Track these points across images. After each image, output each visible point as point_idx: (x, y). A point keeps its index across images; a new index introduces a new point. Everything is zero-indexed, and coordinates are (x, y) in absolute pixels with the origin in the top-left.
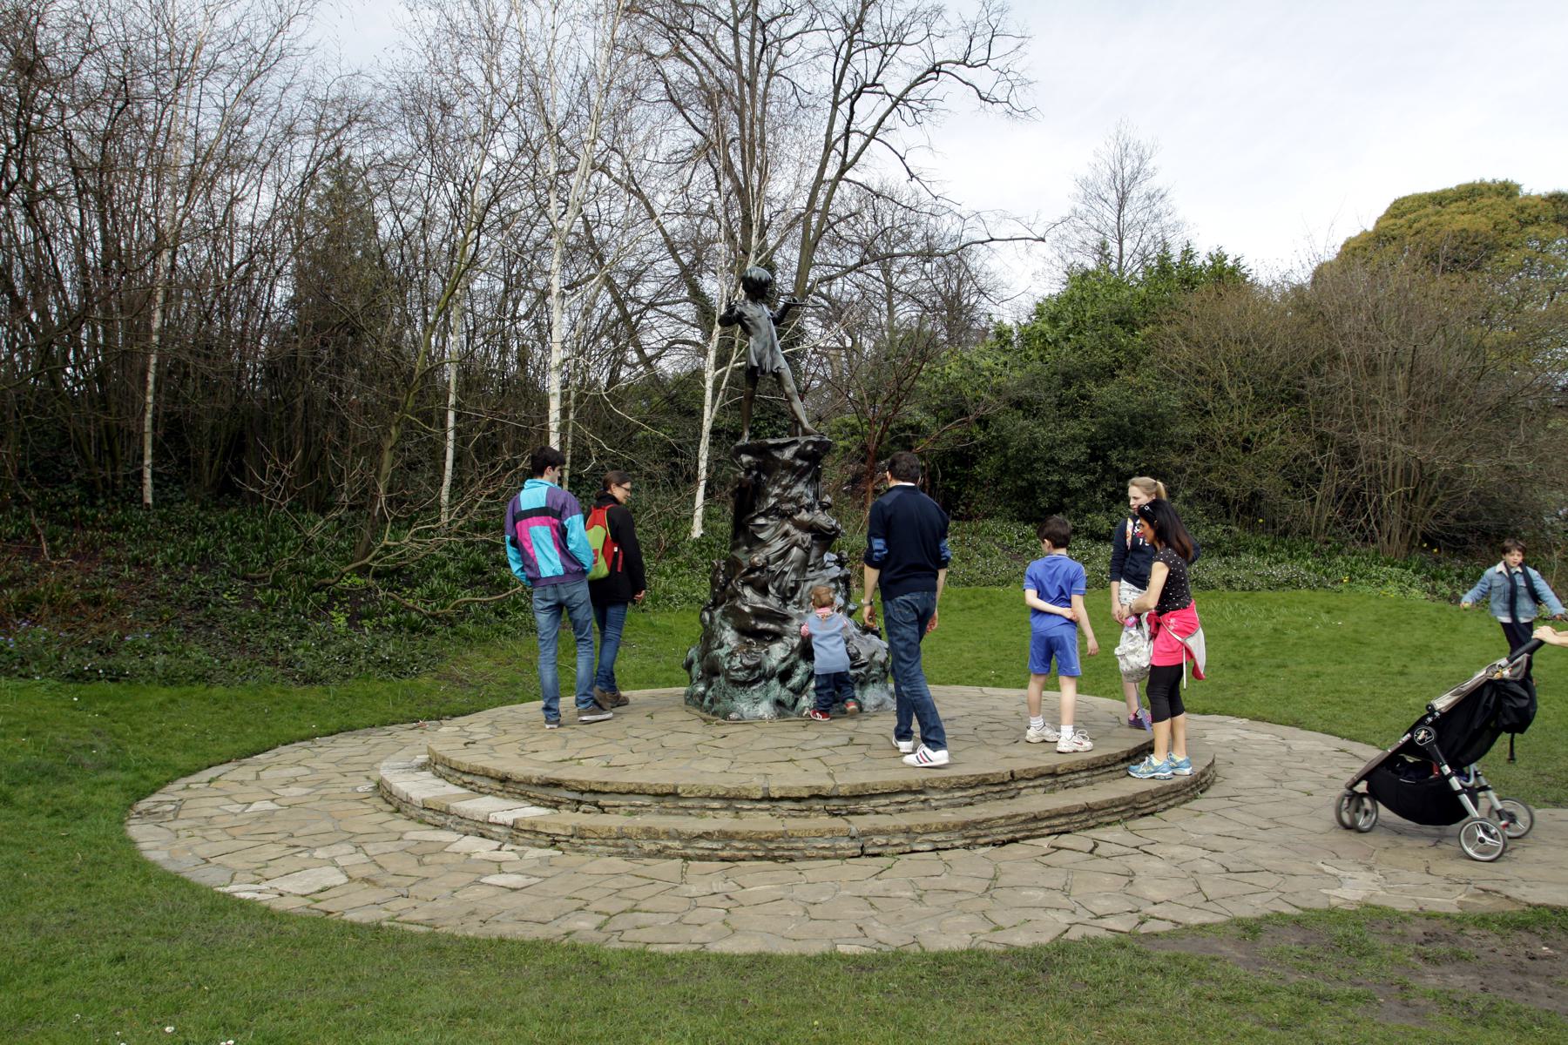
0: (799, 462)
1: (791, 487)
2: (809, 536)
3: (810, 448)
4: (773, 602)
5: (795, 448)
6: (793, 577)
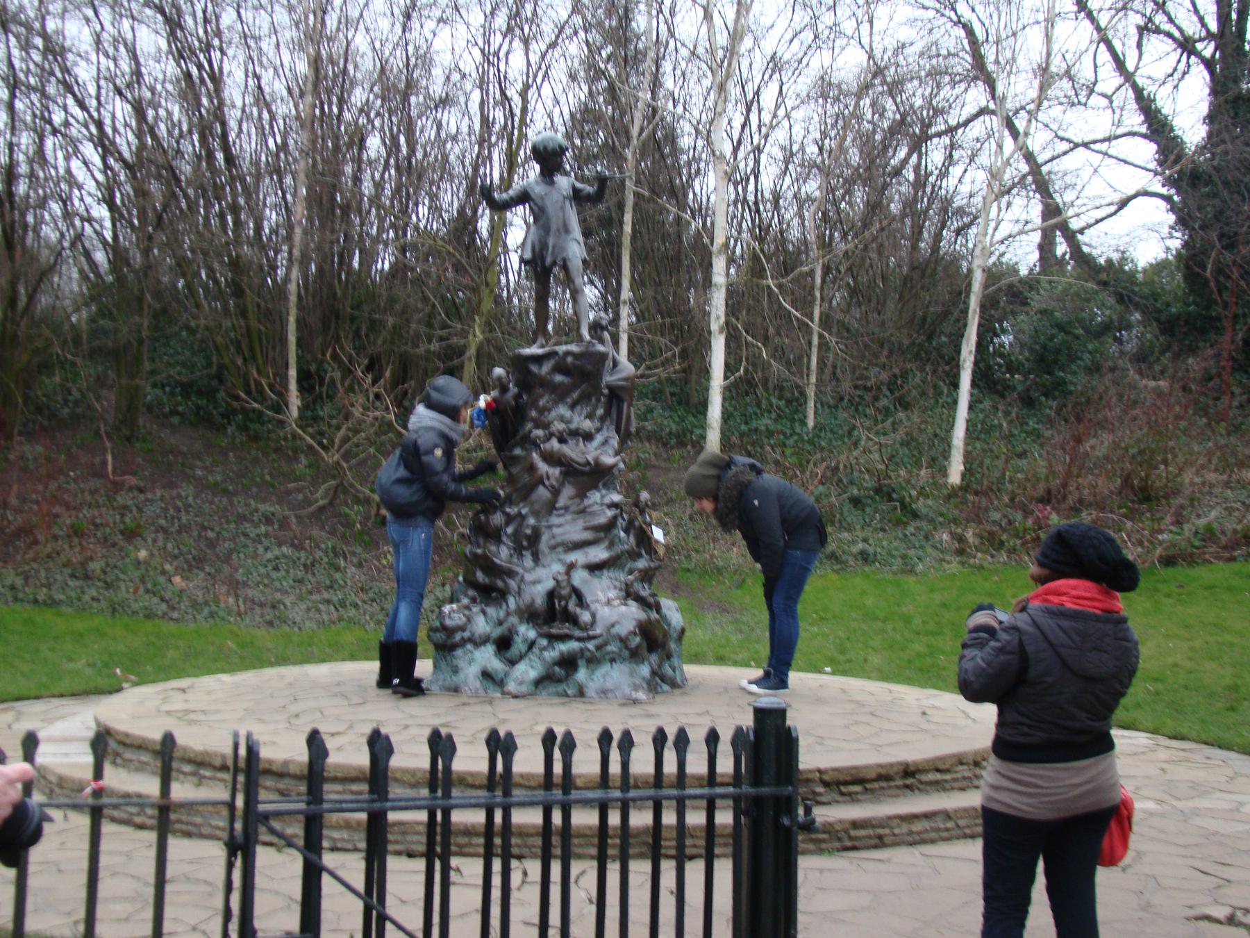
0: (559, 378)
1: (549, 410)
6: (532, 521)
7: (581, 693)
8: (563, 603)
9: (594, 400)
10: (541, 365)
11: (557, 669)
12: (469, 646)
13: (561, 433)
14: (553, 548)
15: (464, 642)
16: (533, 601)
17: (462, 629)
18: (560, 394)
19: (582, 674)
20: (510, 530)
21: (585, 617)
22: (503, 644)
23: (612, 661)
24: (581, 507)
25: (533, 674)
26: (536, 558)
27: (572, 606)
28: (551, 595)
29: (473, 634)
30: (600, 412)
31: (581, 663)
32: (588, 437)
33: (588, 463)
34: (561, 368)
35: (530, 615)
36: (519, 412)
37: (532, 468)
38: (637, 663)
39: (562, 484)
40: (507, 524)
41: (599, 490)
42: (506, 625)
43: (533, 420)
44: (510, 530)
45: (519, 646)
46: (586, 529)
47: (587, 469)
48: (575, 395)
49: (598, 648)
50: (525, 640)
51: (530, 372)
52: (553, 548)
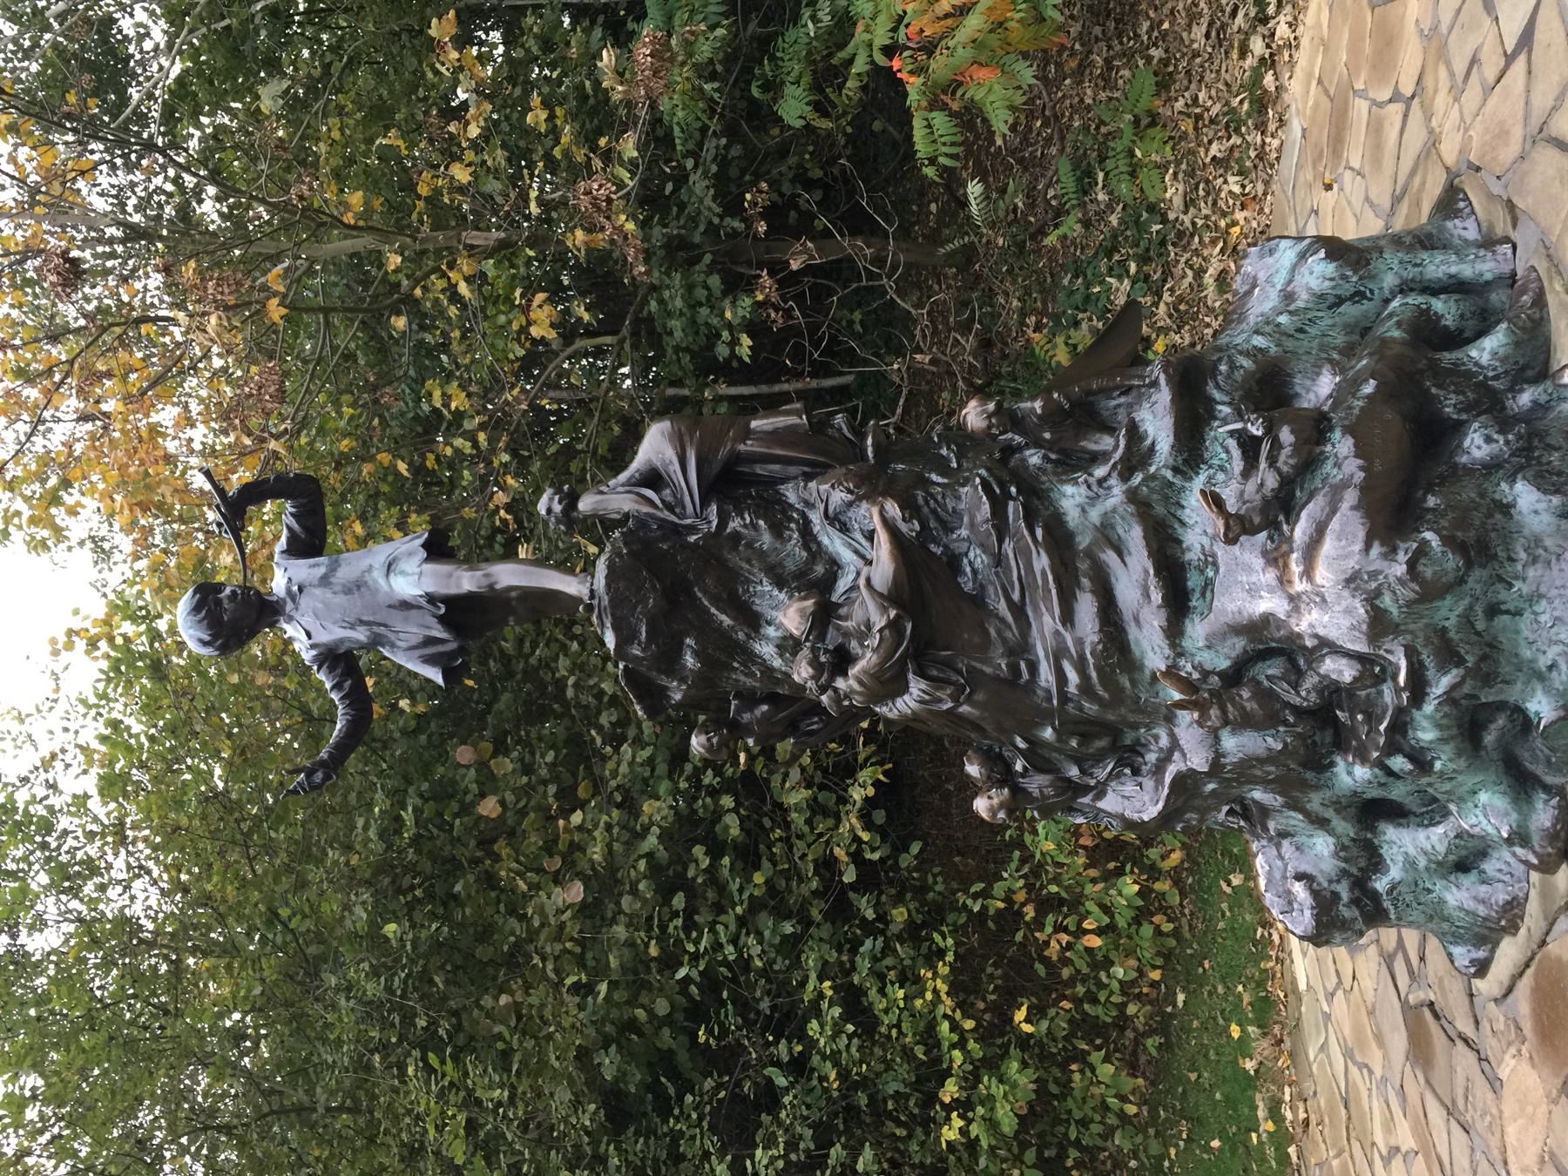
1: (768, 670)
2: (917, 687)
6: (1048, 733)
11: (1490, 738)
18: (726, 652)
21: (1341, 670)
29: (1344, 873)
33: (894, 626)
38: (1507, 538)
42: (1329, 813)
46: (1068, 617)
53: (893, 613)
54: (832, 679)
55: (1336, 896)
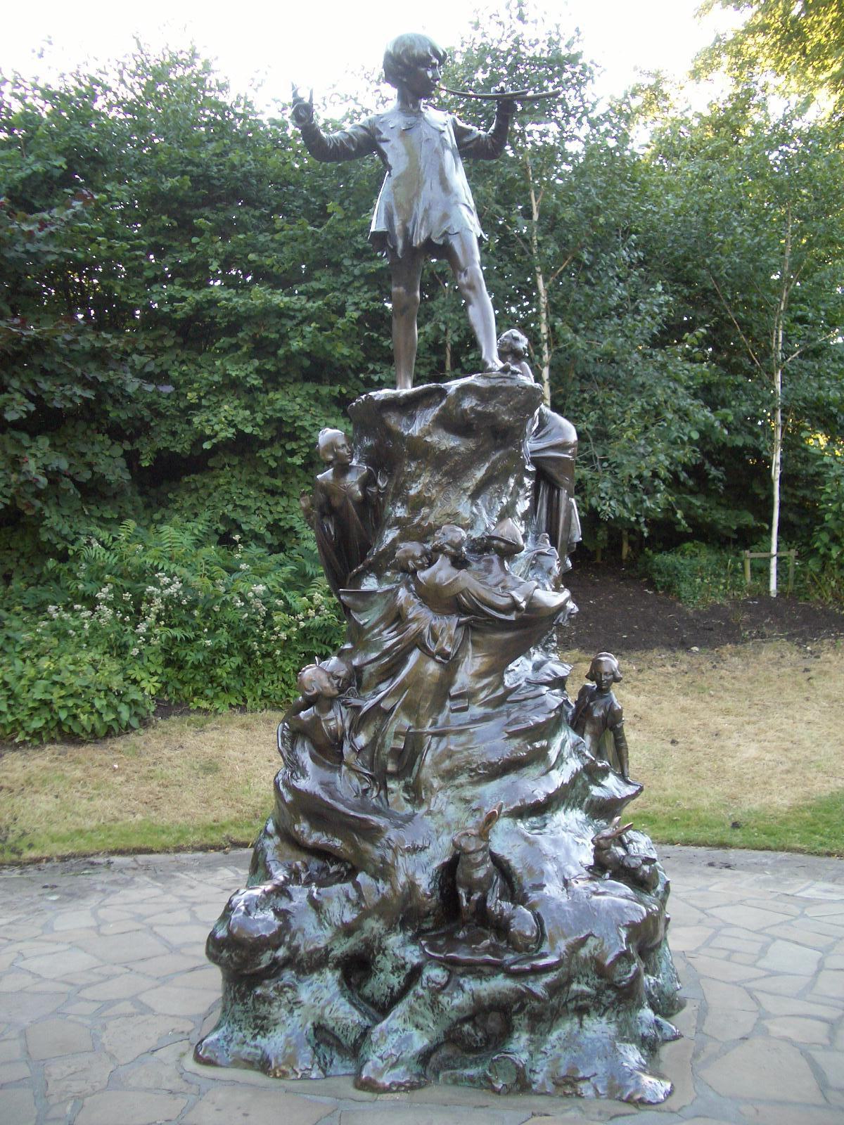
0: (446, 441)
1: (430, 503)
3: (468, 404)
4: (346, 787)
5: (435, 411)
7: (522, 1083)
8: (476, 897)
9: (512, 482)
10: (412, 418)
11: (467, 1027)
12: (288, 975)
13: (457, 546)
14: (450, 775)
15: (276, 968)
16: (412, 886)
17: (273, 942)
18: (451, 469)
19: (520, 1043)
20: (362, 740)
21: (523, 923)
22: (356, 969)
23: (582, 1011)
24: (500, 692)
25: (420, 1042)
26: (416, 793)
27: (498, 905)
28: (450, 873)
30: (523, 506)
31: (520, 1020)
32: (509, 551)
33: (515, 606)
34: (449, 422)
35: (406, 914)
36: (371, 510)
37: (397, 618)
39: (462, 648)
40: (356, 728)
41: (529, 657)
43: (399, 522)
44: (362, 740)
45: (385, 980)
47: (512, 617)
48: (480, 474)
49: (554, 989)
50: (398, 968)
51: (390, 433)
52: (450, 775)
53: (523, 605)
54: (446, 554)
55: (276, 948)
